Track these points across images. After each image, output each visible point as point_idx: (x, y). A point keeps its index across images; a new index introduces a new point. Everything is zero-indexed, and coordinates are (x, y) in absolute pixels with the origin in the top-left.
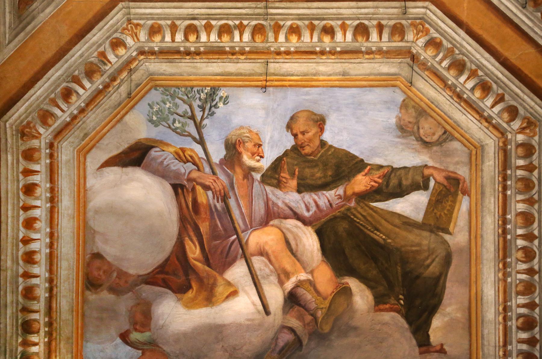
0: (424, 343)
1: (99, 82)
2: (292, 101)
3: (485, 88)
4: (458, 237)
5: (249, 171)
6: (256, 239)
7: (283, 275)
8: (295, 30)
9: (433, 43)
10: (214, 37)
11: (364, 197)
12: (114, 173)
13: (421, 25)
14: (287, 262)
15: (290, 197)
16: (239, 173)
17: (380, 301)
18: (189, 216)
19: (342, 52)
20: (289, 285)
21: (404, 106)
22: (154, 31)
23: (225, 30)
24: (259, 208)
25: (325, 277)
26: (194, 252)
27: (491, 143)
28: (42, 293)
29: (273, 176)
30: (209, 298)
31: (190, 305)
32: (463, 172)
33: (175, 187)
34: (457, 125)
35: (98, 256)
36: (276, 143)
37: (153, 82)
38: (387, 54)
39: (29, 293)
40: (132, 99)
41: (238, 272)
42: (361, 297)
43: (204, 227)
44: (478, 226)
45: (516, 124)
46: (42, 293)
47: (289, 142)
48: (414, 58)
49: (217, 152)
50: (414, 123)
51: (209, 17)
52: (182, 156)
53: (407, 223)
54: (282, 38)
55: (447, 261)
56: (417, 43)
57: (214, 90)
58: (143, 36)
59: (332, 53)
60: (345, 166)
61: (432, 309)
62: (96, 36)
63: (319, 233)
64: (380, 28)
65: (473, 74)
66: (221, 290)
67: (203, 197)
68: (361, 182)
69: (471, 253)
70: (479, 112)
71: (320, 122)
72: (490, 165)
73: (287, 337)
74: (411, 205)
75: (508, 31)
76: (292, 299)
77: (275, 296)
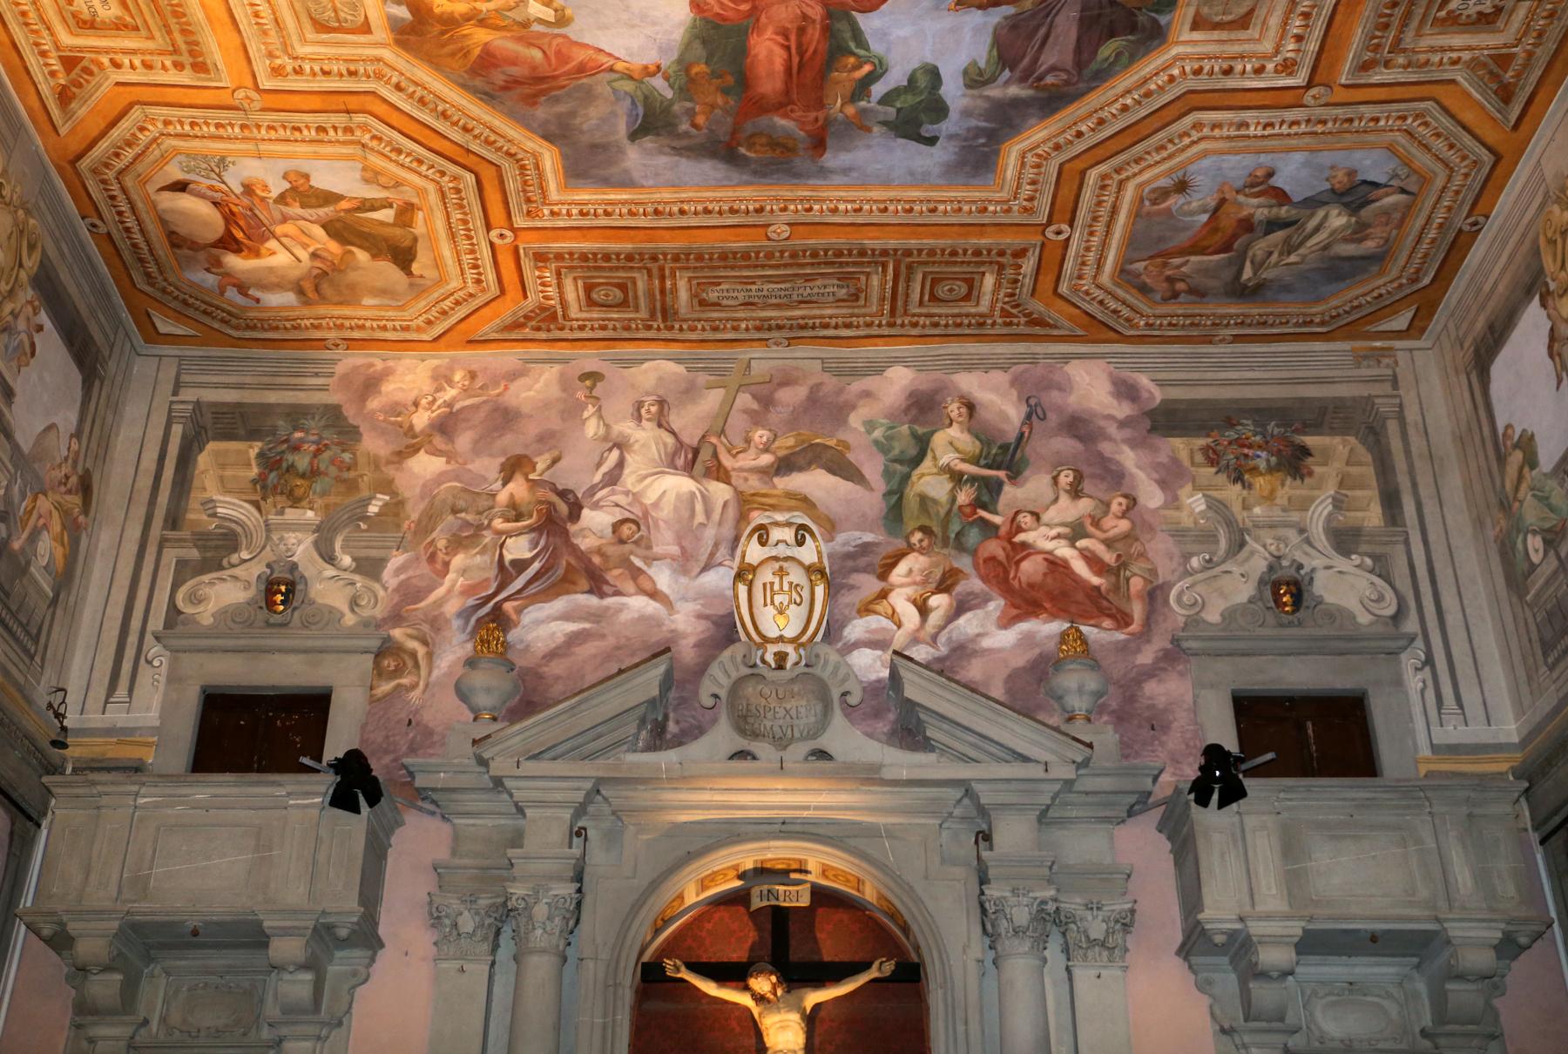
0: (410, 274)
1: (137, 150)
2: (283, 165)
3: (420, 162)
4: (419, 228)
5: (263, 199)
6: (279, 230)
7: (305, 246)
8: (270, 128)
9: (374, 137)
10: (212, 129)
11: (348, 211)
12: (167, 195)
13: (365, 128)
14: (306, 240)
15: (295, 210)
16: (256, 201)
17: (374, 256)
18: (230, 218)
19: (311, 141)
20: (311, 250)
21: (364, 169)
22: (167, 123)
23: (218, 126)
24: (277, 215)
25: (334, 247)
26: (239, 235)
27: (431, 187)
28: (143, 245)
29: (282, 199)
30: (258, 255)
31: (245, 258)
32: (415, 200)
33: (215, 204)
34: (405, 179)
35: (173, 233)
36: (277, 187)
37: (177, 152)
38: (344, 143)
39: (135, 246)
40: (164, 159)
41: (272, 244)
42: (362, 256)
43: (242, 223)
44: (430, 224)
45: (446, 179)
46: (143, 245)
47: (288, 186)
48: (363, 146)
49: (238, 190)
50: (372, 176)
51: (205, 118)
52: (211, 188)
53: (382, 223)
54: (263, 131)
55: (415, 240)
56: (366, 138)
57: (223, 159)
58: (160, 125)
59: (303, 141)
60: (329, 198)
61: (412, 261)
62: (125, 124)
63: (323, 227)
64: (335, 128)
65: (408, 155)
66: (263, 251)
67: (234, 209)
68: (344, 205)
69: (431, 237)
70: (420, 174)
71: (307, 177)
72: (433, 197)
73: (316, 272)
74: (386, 215)
75: (428, 132)
76: (314, 255)
77: (304, 255)
